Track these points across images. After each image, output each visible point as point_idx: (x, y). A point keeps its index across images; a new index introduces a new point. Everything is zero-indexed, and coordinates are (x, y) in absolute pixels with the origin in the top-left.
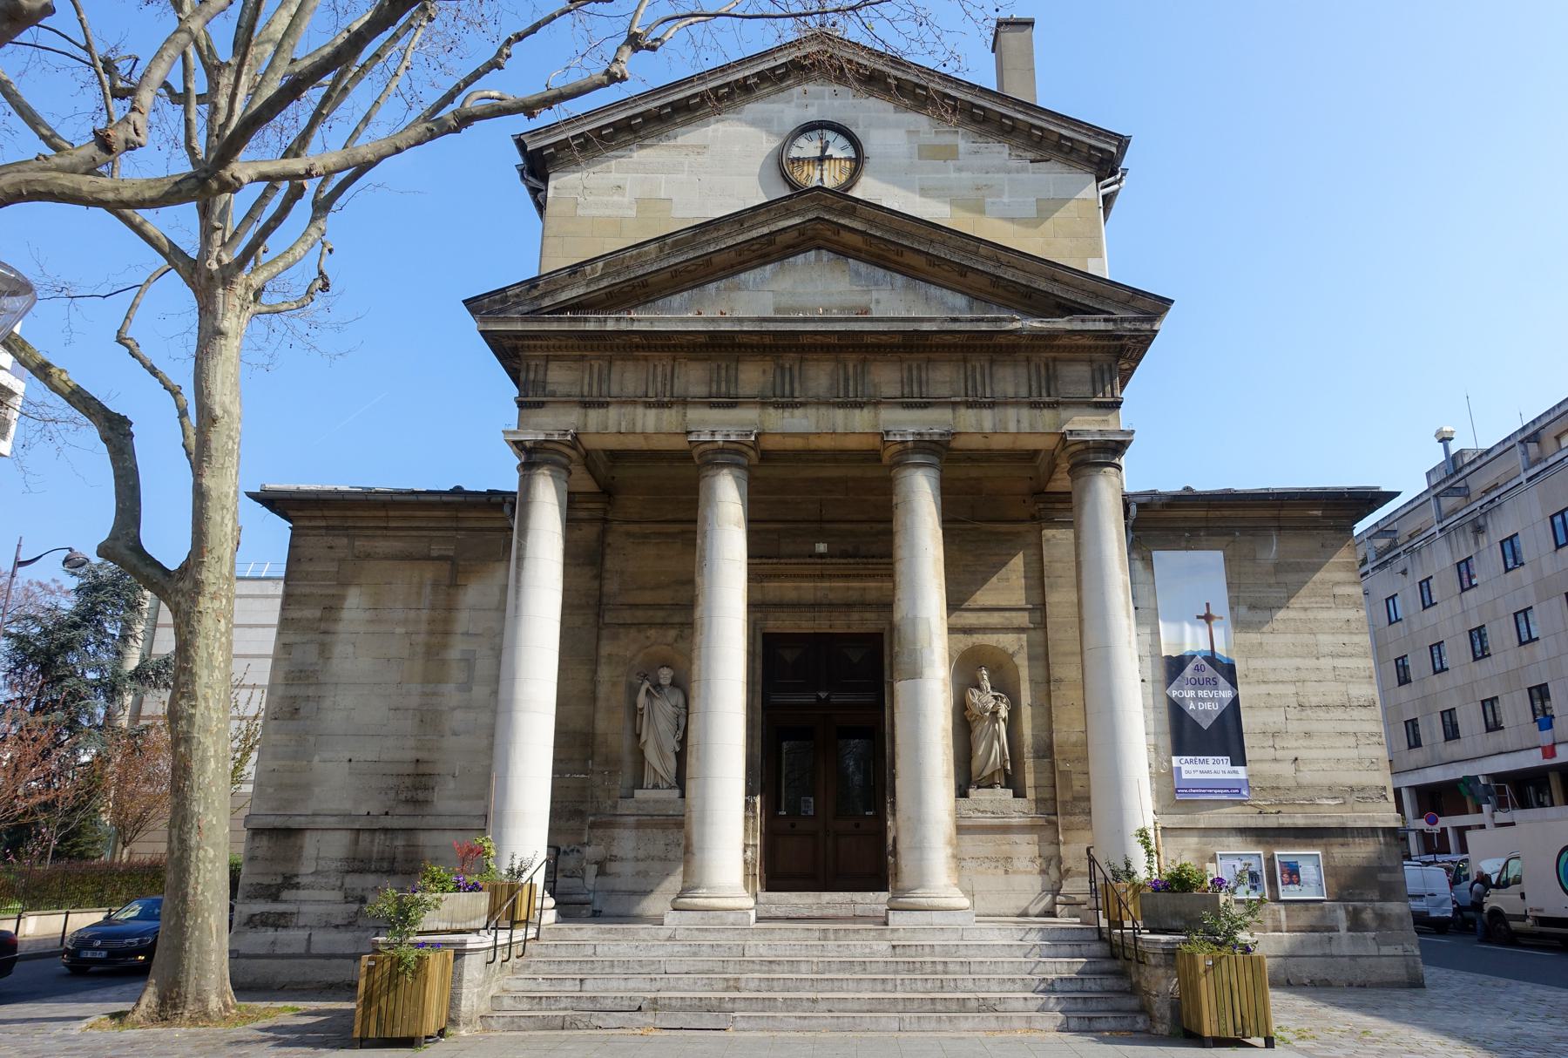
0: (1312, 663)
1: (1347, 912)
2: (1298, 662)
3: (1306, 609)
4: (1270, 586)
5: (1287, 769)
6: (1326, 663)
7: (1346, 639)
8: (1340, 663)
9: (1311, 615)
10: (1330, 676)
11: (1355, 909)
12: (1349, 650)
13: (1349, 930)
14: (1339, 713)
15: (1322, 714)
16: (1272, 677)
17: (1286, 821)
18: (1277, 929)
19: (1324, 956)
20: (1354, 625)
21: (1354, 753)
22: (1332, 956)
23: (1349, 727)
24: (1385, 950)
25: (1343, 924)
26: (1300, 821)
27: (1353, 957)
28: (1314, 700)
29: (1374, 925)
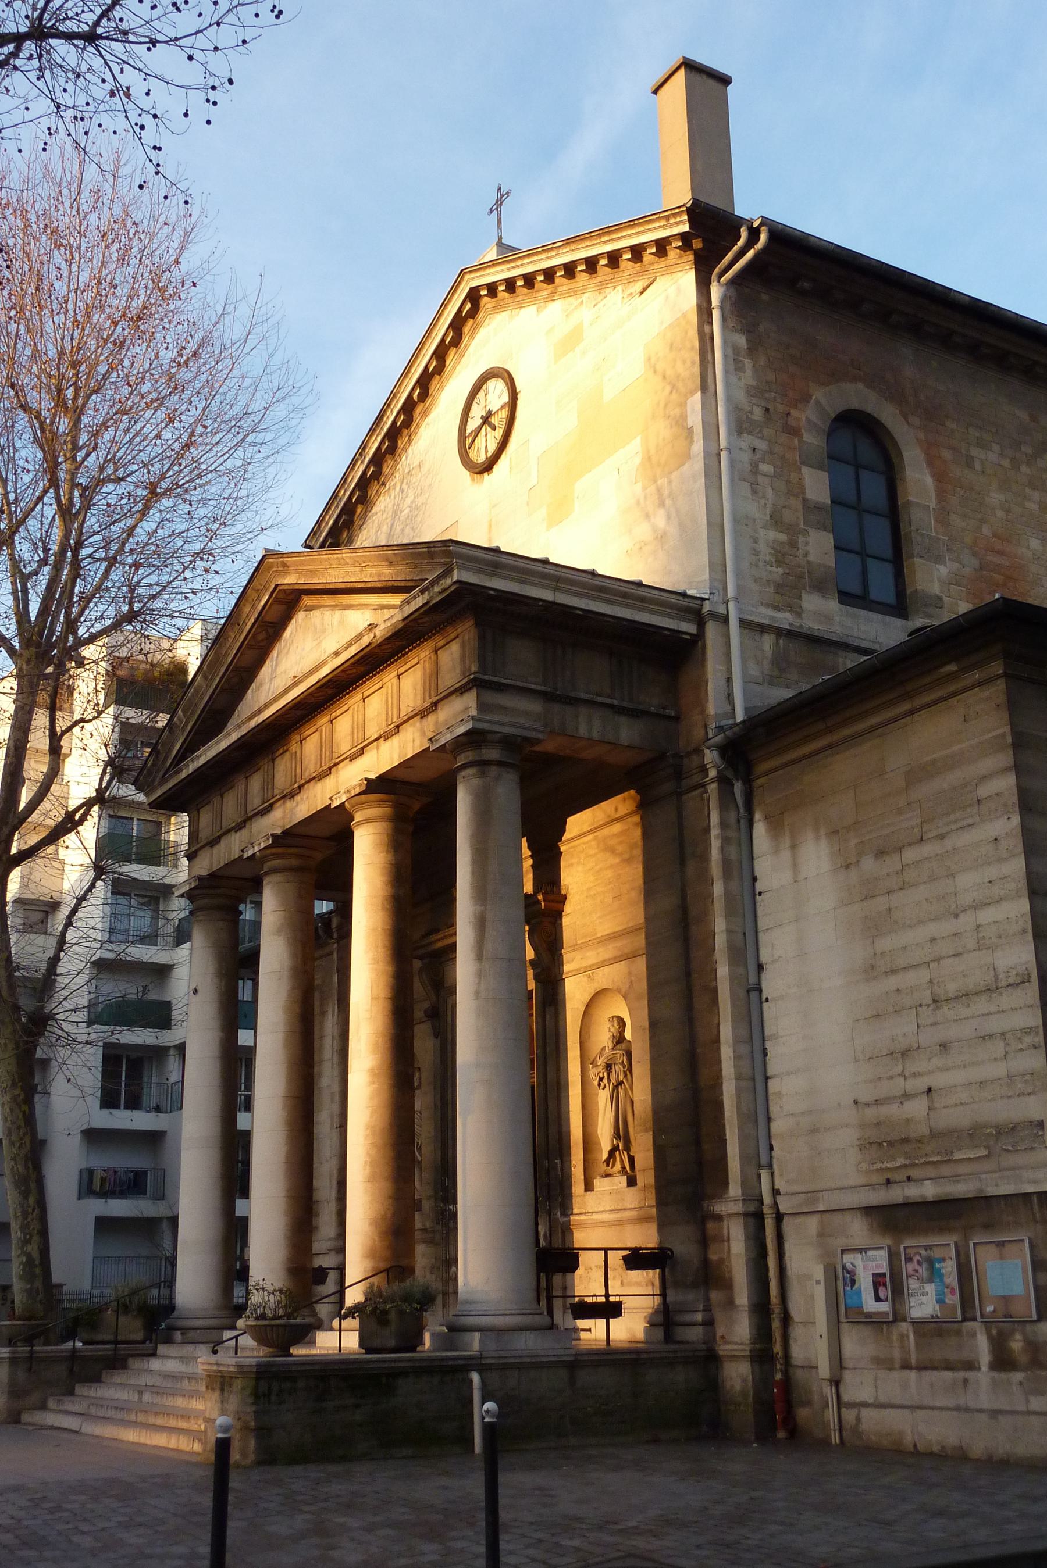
0: (948, 926)
2: (932, 929)
3: (942, 837)
4: (900, 811)
5: (917, 1108)
6: (967, 920)
8: (986, 916)
9: (949, 843)
10: (971, 944)
11: (1000, 1333)
14: (982, 1005)
15: (963, 1011)
16: (902, 962)
17: (914, 1192)
18: (906, 1366)
19: (957, 1409)
21: (1000, 1070)
22: (967, 1410)
23: (995, 1025)
25: (985, 1358)
26: (929, 1191)
28: (952, 988)
29: (1024, 1359)
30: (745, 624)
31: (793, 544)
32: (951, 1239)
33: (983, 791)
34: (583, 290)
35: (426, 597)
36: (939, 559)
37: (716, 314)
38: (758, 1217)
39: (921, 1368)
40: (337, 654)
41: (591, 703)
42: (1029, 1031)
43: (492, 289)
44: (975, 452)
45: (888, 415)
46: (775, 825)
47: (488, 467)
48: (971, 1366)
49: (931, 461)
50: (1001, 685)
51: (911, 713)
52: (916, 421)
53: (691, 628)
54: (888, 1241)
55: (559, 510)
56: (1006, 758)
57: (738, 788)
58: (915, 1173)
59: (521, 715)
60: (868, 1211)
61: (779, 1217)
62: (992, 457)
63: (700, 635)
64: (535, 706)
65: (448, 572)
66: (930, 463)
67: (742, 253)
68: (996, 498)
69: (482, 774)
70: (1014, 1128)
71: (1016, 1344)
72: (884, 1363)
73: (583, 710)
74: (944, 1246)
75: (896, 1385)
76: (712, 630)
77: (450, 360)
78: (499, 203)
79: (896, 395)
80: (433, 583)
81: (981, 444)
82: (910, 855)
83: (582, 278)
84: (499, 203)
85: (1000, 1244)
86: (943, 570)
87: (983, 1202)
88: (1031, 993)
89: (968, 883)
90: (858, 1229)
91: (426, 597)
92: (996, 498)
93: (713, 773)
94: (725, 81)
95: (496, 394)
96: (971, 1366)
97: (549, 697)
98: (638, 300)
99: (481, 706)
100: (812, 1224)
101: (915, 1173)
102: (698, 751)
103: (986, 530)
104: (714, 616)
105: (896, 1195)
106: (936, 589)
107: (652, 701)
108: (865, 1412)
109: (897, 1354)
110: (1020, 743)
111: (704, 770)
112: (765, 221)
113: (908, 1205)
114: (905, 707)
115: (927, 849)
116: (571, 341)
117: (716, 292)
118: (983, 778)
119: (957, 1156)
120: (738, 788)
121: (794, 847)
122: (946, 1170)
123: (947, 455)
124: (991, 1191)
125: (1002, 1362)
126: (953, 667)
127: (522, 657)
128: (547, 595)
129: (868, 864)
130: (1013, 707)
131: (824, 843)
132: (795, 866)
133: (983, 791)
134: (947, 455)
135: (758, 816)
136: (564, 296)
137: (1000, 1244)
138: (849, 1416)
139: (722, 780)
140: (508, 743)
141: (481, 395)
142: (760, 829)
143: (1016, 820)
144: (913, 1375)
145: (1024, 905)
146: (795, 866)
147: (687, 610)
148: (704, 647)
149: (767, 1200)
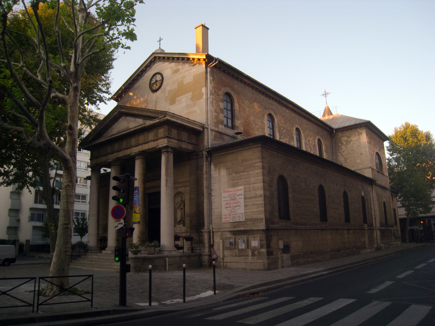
1: (251, 252)
6: (251, 186)
7: (257, 178)
8: (255, 185)
9: (249, 173)
12: (257, 181)
13: (252, 256)
14: (253, 199)
17: (239, 229)
18: (236, 256)
20: (259, 174)
21: (256, 210)
22: (247, 262)
23: (256, 203)
24: (259, 261)
25: (250, 255)
26: (242, 229)
27: (251, 263)
28: (248, 196)
30: (211, 129)
31: (218, 116)
32: (246, 236)
33: (256, 165)
34: (180, 62)
35: (159, 120)
36: (239, 120)
37: (208, 73)
38: (210, 232)
39: (239, 256)
40: (136, 127)
41: (185, 141)
42: (262, 204)
43: (159, 58)
44: (244, 101)
45: (232, 93)
46: (216, 166)
47: (156, 91)
48: (248, 256)
49: (238, 102)
50: (260, 148)
51: (243, 150)
52: (236, 95)
53: (201, 129)
54: (234, 237)
55: (173, 102)
56: (260, 160)
57: (209, 158)
58: (240, 226)
59: (174, 143)
60: (230, 231)
61: (213, 232)
62: (247, 102)
63: (203, 131)
64: (176, 142)
65: (165, 117)
66: (238, 103)
67: (213, 63)
68: (247, 109)
69: (168, 154)
70: (258, 219)
71: (256, 252)
72: (232, 256)
73: (183, 143)
74: (245, 237)
75: (233, 259)
76: (206, 130)
77: (148, 69)
78: (160, 40)
79: (233, 90)
80: (161, 118)
81: (246, 100)
82: (241, 174)
83: (179, 61)
84: (160, 40)
85: (254, 237)
86: (239, 122)
87: (252, 231)
88: (262, 198)
89: (252, 180)
90: (228, 235)
91: (159, 120)
92: (247, 109)
93: (205, 156)
94: (208, 29)
95: (159, 77)
96: (248, 256)
97: (178, 140)
98: (192, 67)
99: (168, 141)
100: (220, 234)
101: (240, 226)
102: (202, 151)
103: (246, 115)
104: (206, 128)
105: (236, 229)
106: (238, 125)
107: (194, 141)
108: (228, 263)
109: (234, 254)
110: (263, 158)
111: (203, 155)
112: (218, 59)
113: (238, 231)
114: (243, 149)
115: (245, 173)
116: (177, 71)
117: (209, 70)
118: (256, 163)
119: (248, 223)
120: (209, 158)
121: (219, 170)
122: (245, 225)
123: (241, 101)
124: (253, 229)
125: (253, 255)
126: (252, 144)
127: (174, 132)
128: (180, 122)
129: (234, 174)
130: (262, 152)
131: (225, 170)
132: (219, 173)
133: (256, 165)
134: (241, 101)
135: (212, 164)
136: (175, 62)
137: (254, 237)
138: (225, 264)
139: (207, 157)
140: (172, 148)
141: (155, 77)
142: (212, 166)
143: (261, 170)
144: (237, 258)
145: (262, 184)
146: (219, 173)
147: (202, 126)
148: (204, 133)
149: (211, 229)
